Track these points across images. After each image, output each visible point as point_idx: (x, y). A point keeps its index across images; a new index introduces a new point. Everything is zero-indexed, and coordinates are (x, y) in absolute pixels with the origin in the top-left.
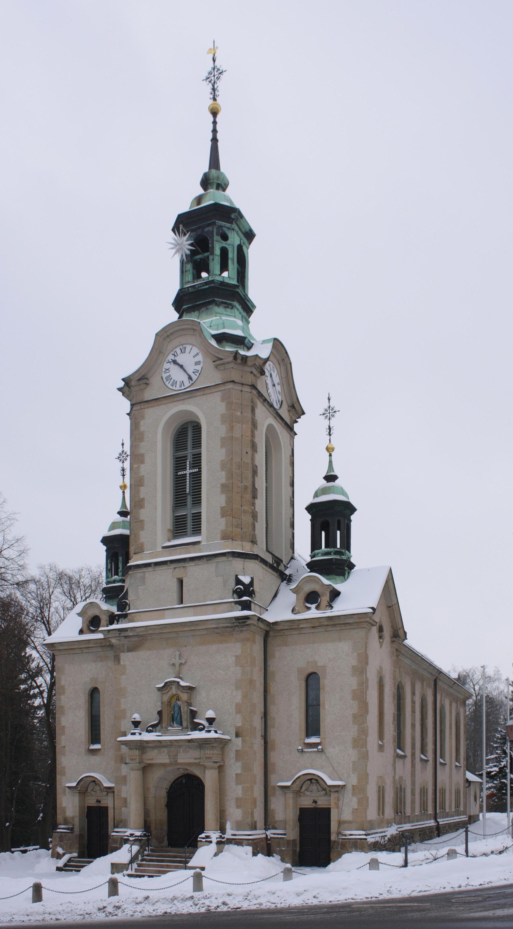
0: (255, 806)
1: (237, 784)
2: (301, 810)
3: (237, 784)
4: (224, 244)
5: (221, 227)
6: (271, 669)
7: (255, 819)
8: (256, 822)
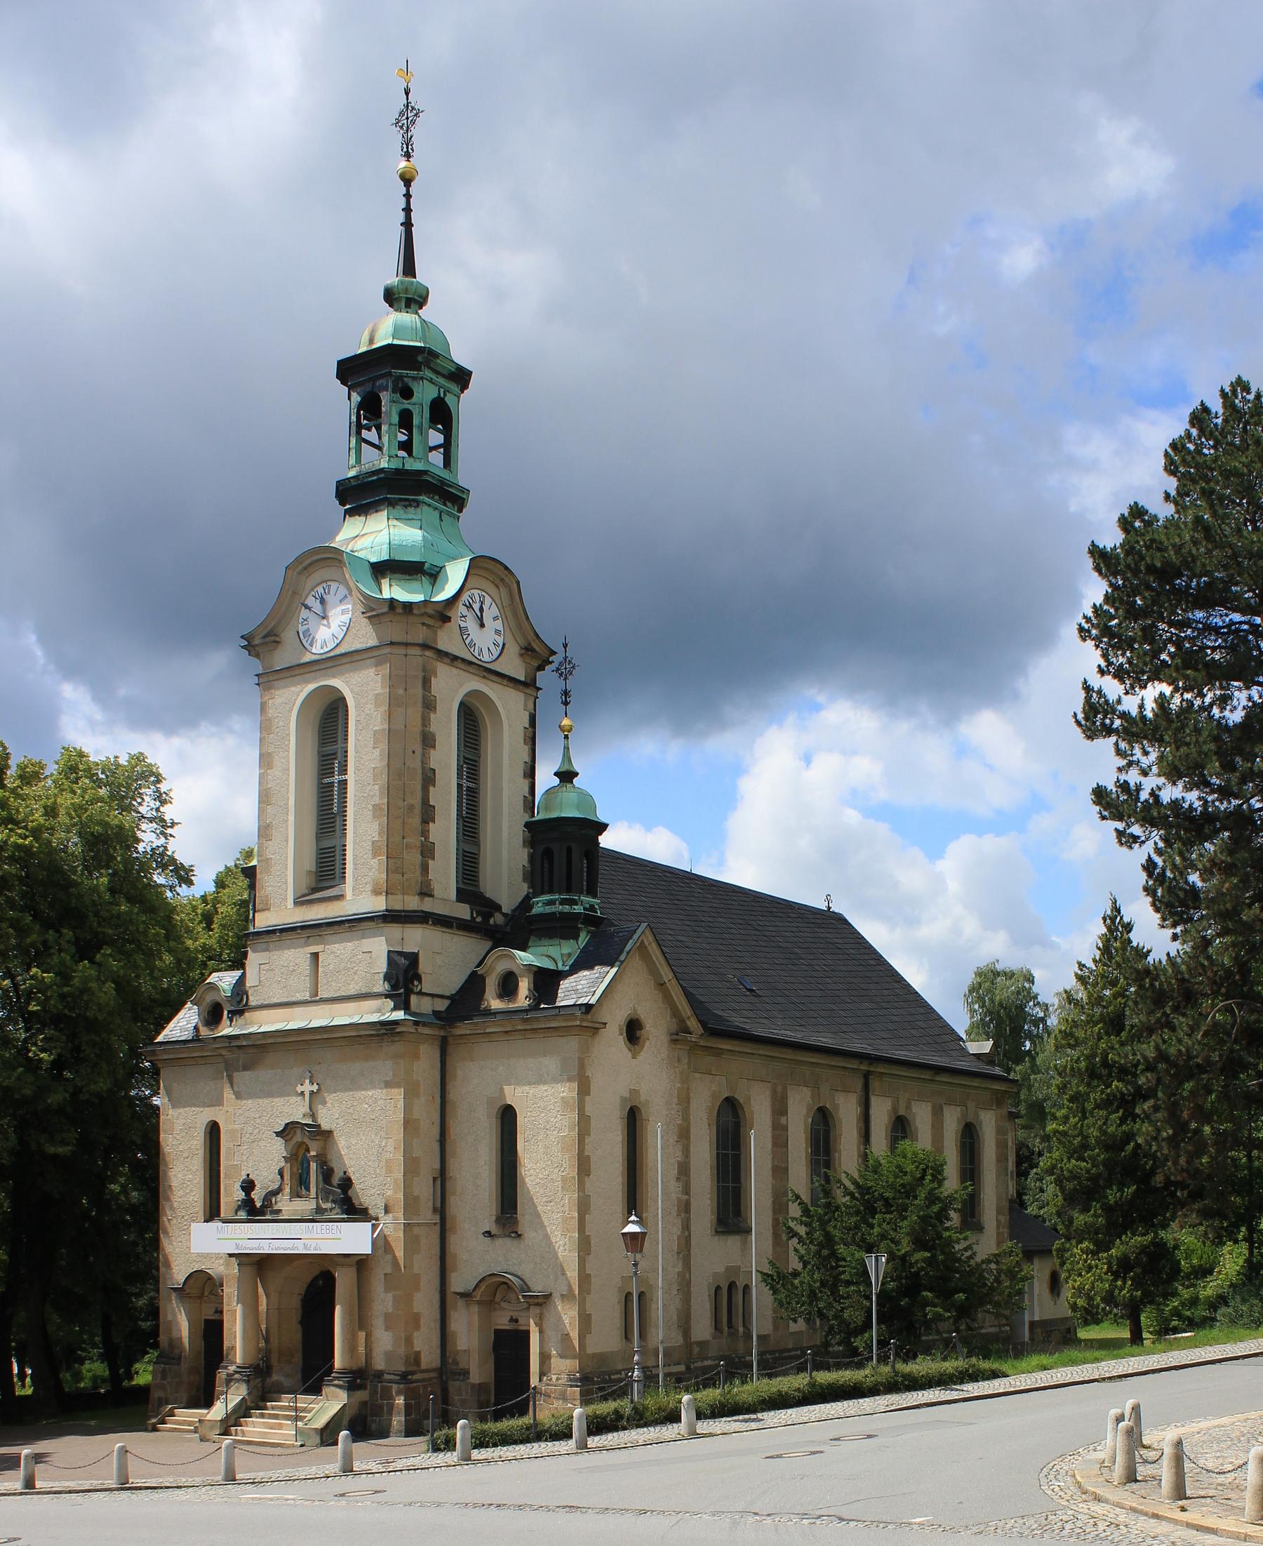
0: (417, 1326)
1: (387, 1290)
2: (498, 1332)
3: (387, 1290)
4: (406, 404)
5: (401, 377)
6: (452, 1095)
7: (417, 1349)
8: (418, 1354)
